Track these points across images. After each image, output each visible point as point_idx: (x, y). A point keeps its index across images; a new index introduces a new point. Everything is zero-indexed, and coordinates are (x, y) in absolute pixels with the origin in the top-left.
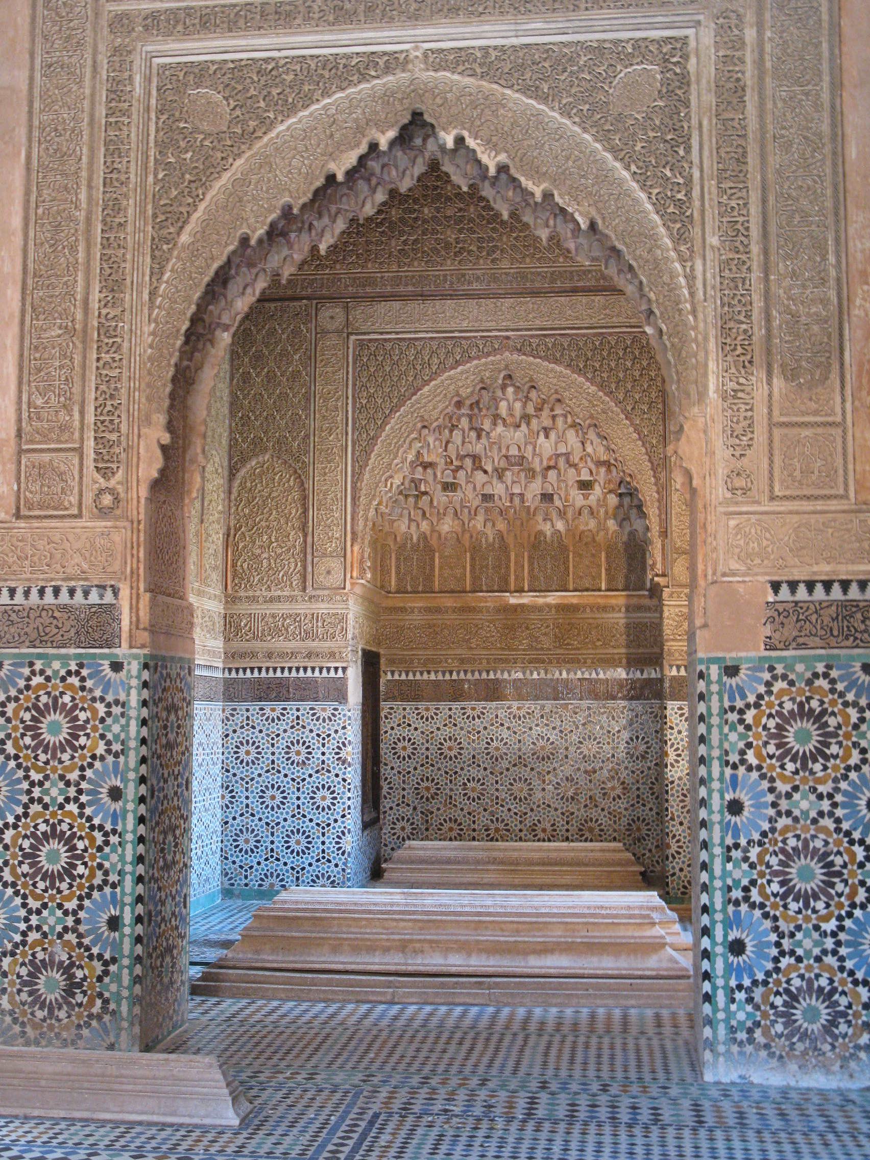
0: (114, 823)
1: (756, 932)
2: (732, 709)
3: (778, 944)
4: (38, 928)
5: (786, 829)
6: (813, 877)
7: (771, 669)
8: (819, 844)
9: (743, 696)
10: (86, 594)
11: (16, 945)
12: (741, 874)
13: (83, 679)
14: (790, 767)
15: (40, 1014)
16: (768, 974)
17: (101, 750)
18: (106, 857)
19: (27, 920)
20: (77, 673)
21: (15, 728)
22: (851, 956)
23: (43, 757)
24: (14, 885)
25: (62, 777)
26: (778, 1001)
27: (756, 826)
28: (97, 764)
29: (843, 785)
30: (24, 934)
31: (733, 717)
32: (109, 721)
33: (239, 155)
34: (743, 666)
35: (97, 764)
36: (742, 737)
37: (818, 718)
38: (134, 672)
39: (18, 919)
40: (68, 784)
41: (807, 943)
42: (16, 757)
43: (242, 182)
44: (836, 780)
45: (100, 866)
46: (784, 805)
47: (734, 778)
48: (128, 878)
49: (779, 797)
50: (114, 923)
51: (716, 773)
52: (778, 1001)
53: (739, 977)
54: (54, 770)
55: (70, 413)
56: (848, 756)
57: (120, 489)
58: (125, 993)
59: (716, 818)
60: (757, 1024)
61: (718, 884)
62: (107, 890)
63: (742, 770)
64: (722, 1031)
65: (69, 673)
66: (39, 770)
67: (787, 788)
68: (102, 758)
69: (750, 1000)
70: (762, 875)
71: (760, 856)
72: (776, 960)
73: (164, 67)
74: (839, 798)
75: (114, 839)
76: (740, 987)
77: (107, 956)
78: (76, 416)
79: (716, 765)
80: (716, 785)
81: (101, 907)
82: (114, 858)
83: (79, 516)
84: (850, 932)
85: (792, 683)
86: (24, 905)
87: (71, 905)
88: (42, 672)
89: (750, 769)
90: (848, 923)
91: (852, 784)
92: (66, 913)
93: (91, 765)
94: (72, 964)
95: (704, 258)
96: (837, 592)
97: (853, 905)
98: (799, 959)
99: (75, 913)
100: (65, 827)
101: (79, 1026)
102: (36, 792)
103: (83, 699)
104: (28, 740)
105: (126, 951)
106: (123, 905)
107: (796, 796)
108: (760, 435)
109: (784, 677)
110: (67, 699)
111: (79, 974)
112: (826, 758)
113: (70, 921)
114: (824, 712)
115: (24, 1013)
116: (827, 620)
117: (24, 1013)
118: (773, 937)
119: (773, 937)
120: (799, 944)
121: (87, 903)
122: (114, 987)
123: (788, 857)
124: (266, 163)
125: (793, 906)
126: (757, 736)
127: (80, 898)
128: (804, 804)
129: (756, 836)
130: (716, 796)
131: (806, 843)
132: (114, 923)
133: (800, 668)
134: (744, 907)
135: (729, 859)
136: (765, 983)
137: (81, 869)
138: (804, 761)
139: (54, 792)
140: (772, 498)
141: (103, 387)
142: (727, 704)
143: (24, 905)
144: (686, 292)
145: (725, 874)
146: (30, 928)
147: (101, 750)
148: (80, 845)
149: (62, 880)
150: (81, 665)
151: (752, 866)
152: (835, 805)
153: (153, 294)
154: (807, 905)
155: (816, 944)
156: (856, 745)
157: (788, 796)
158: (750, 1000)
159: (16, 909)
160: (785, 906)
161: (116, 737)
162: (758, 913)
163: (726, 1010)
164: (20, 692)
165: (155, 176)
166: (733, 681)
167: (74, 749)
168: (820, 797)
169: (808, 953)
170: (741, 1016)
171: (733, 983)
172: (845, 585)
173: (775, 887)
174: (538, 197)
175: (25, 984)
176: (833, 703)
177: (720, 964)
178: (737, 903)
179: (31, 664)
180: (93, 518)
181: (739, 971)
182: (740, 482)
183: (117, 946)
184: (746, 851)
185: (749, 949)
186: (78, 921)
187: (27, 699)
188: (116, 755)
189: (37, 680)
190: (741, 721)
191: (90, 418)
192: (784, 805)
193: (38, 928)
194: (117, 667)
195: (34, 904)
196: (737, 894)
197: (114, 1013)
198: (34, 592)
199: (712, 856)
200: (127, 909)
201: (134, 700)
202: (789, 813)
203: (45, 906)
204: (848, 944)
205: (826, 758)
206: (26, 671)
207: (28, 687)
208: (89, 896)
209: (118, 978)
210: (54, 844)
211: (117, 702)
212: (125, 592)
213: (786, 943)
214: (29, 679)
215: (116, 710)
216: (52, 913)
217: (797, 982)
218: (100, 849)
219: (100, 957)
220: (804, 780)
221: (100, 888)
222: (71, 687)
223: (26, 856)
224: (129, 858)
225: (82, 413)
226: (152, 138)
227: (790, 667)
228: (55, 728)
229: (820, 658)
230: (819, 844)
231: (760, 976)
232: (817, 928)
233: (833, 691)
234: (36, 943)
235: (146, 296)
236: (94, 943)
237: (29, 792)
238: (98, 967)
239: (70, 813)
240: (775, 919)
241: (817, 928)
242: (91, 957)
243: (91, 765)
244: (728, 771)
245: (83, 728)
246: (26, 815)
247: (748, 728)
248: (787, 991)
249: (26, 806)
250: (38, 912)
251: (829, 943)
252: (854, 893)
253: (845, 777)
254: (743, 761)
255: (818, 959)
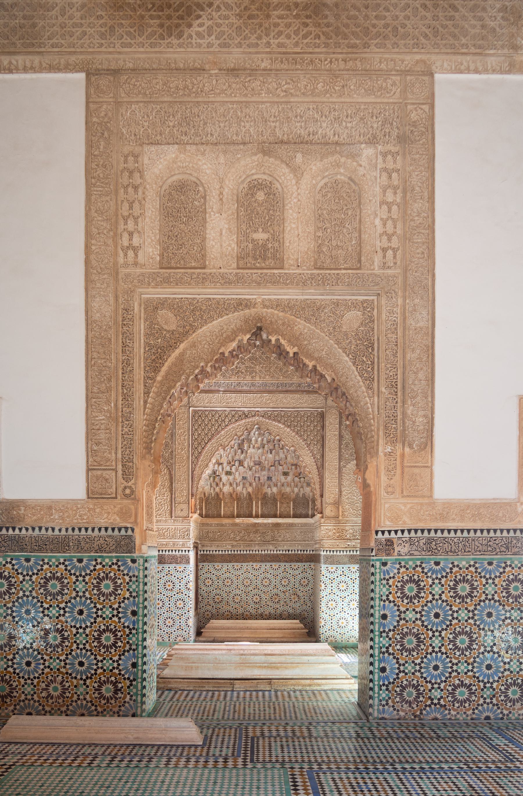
0: (134, 625)
1: (391, 664)
2: (384, 579)
3: (399, 668)
4: (102, 668)
5: (403, 625)
6: (412, 643)
7: (400, 563)
8: (415, 630)
9: (389, 574)
10: (120, 530)
11: (92, 675)
12: (385, 642)
13: (119, 566)
14: (406, 601)
15: (103, 702)
16: (395, 679)
17: (127, 595)
18: (131, 639)
19: (97, 664)
20: (116, 564)
21: (90, 587)
22: (425, 672)
23: (102, 599)
24: (91, 650)
25: (111, 607)
26: (398, 689)
27: (392, 624)
28: (126, 601)
29: (425, 608)
30: (96, 670)
31: (384, 582)
32: (131, 583)
33: (182, 342)
34: (389, 563)
35: (126, 601)
36: (388, 590)
37: (417, 583)
38: (141, 563)
39: (93, 664)
40: (113, 609)
41: (409, 668)
42: (90, 599)
43: (182, 354)
44: (423, 606)
45: (128, 642)
46: (403, 616)
47: (384, 605)
48: (140, 647)
49: (401, 612)
50: (134, 665)
51: (377, 604)
52: (398, 689)
53: (384, 681)
54: (107, 604)
55: (110, 453)
56: (427, 597)
57: (133, 486)
58: (139, 693)
59: (377, 621)
60: (390, 698)
61: (377, 646)
62: (131, 652)
63: (387, 602)
64: (376, 701)
65: (113, 564)
66: (100, 604)
67: (404, 609)
68: (128, 599)
69: (387, 689)
70: (393, 642)
71: (393, 635)
72: (397, 674)
73: (148, 300)
74: (423, 613)
75: (134, 632)
76: (384, 685)
77: (131, 678)
78: (114, 455)
79: (377, 600)
80: (377, 608)
81: (128, 659)
82: (134, 639)
83: (116, 498)
84: (426, 663)
85: (407, 569)
86: (95, 659)
87: (116, 658)
88: (101, 563)
89: (390, 602)
90: (425, 660)
91: (429, 608)
92: (114, 661)
93: (123, 602)
94: (117, 682)
95: (378, 397)
96: (426, 533)
97: (427, 653)
98: (406, 674)
99: (117, 661)
100: (112, 627)
101: (120, 706)
102: (100, 613)
103: (119, 575)
104: (95, 592)
105: (140, 676)
106: (138, 658)
107: (408, 613)
108: (399, 471)
109: (405, 567)
110: (112, 574)
111: (120, 685)
112: (419, 598)
113: (115, 665)
114: (419, 580)
115: (96, 702)
116: (421, 544)
117: (96, 702)
118: (397, 666)
119: (397, 666)
120: (407, 668)
121: (122, 657)
122: (135, 691)
123: (404, 635)
124: (193, 345)
125: (405, 654)
126: (393, 589)
127: (120, 655)
128: (410, 615)
129: (392, 628)
130: (377, 612)
131: (410, 630)
132: (134, 665)
133: (411, 563)
134: (386, 655)
135: (381, 637)
136: (393, 683)
137: (120, 644)
138: (411, 599)
139: (107, 613)
140: (403, 497)
141: (125, 443)
142: (382, 577)
143: (95, 659)
144: (370, 410)
145: (380, 642)
146: (98, 668)
147: (127, 595)
148: (119, 634)
149: (112, 648)
150: (118, 561)
151: (390, 639)
152: (422, 616)
153: (145, 402)
154: (410, 654)
155: (413, 668)
156: (431, 593)
157: (405, 612)
158: (387, 689)
159: (92, 660)
160: (402, 654)
161: (134, 590)
162: (391, 657)
163: (378, 693)
164: (91, 571)
165: (145, 348)
166: (385, 568)
167: (116, 595)
168: (416, 613)
169: (410, 671)
170: (384, 695)
171: (381, 683)
172: (429, 531)
173: (398, 647)
174: (310, 367)
175: (96, 690)
176: (423, 577)
177: (376, 677)
178: (384, 653)
179: (96, 560)
180: (122, 499)
181: (384, 678)
182: (390, 489)
183: (136, 674)
184: (387, 633)
185: (388, 670)
186: (119, 665)
187: (95, 574)
188: (134, 597)
189: (98, 567)
190: (388, 583)
191: (119, 456)
192: (403, 616)
193: (102, 668)
194: (134, 561)
195: (100, 658)
196: (384, 650)
197: (134, 701)
198: (96, 530)
199: (375, 636)
200: (140, 659)
201: (141, 575)
202: (404, 619)
203: (104, 659)
204: (425, 668)
205: (419, 598)
206: (94, 563)
207: (95, 570)
208: (123, 654)
209: (136, 687)
210: (108, 634)
211: (134, 576)
212: (137, 530)
213: (402, 668)
214: (95, 566)
215: (134, 579)
216: (108, 662)
217: (405, 682)
218: (128, 635)
219: (128, 678)
220: (411, 606)
221: (128, 651)
222: (114, 569)
223: (95, 639)
224: (140, 639)
225: (116, 453)
226: (142, 332)
227: (407, 563)
228: (107, 587)
229: (418, 559)
230: (415, 630)
231: (391, 680)
232: (413, 662)
233: (423, 572)
234: (101, 674)
235: (142, 403)
236: (126, 673)
237: (96, 613)
238: (128, 683)
239: (115, 621)
240: (398, 659)
241: (413, 662)
242: (125, 679)
243: (123, 602)
244: (382, 603)
245: (120, 586)
246: (95, 622)
247: (390, 586)
248: (401, 686)
249: (95, 619)
250: (102, 661)
251: (418, 668)
252: (427, 649)
253: (426, 605)
254: (388, 599)
255: (413, 674)
